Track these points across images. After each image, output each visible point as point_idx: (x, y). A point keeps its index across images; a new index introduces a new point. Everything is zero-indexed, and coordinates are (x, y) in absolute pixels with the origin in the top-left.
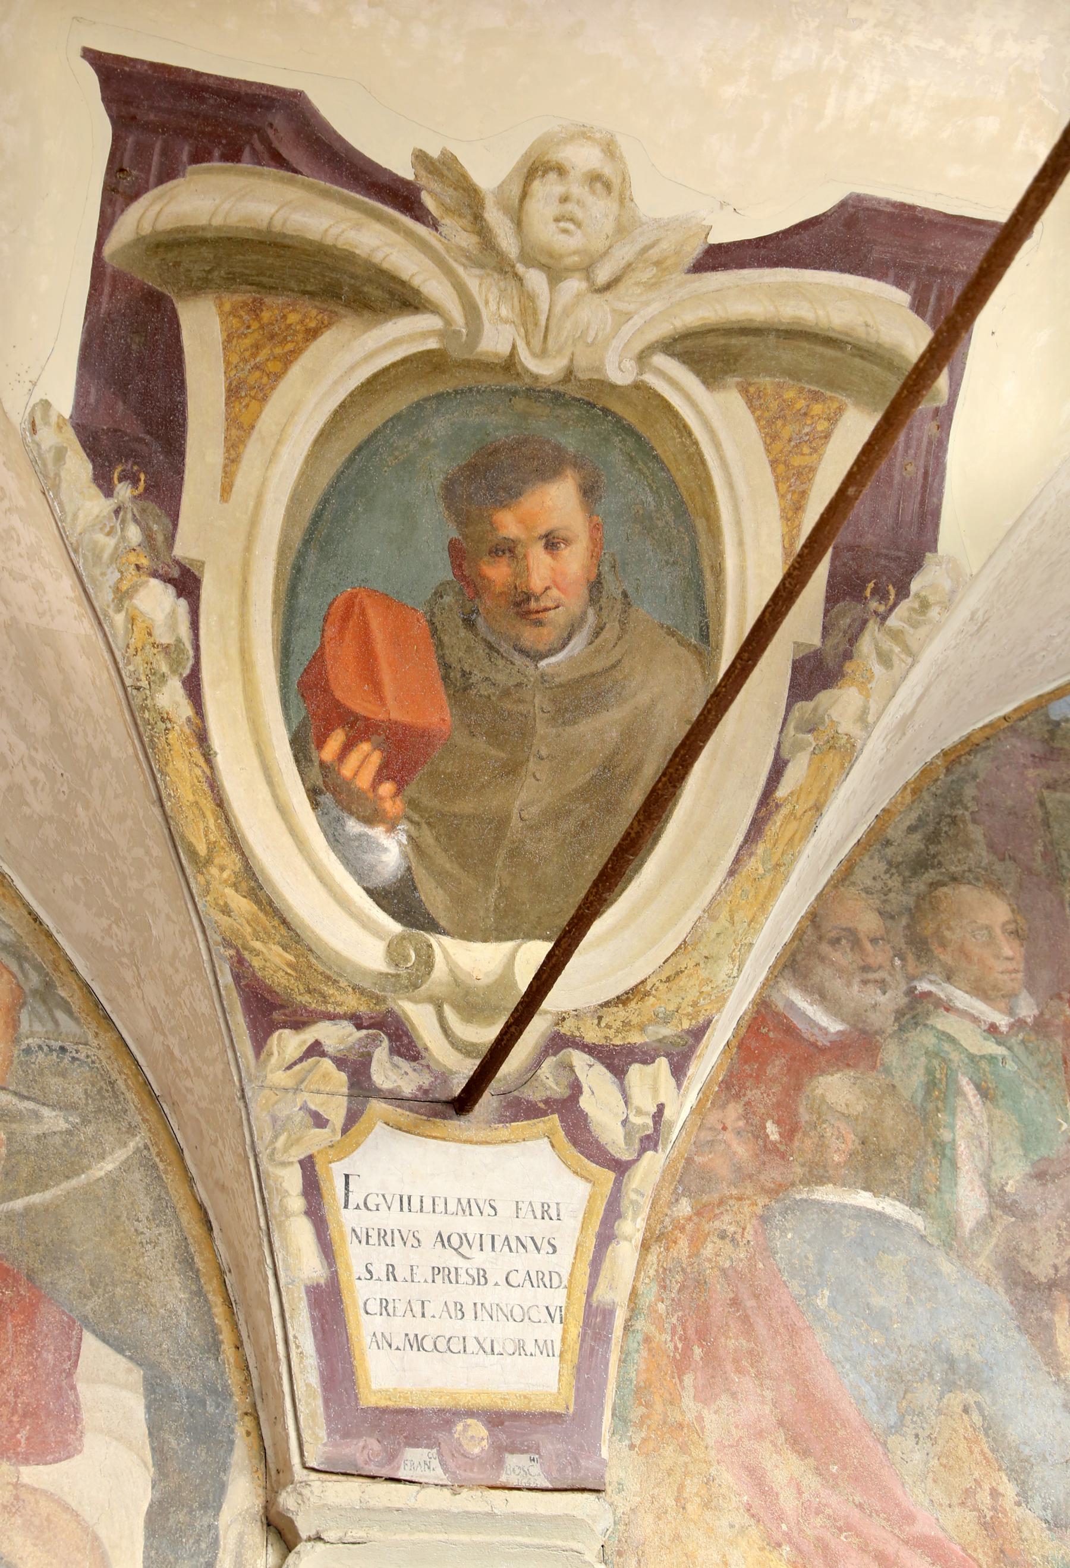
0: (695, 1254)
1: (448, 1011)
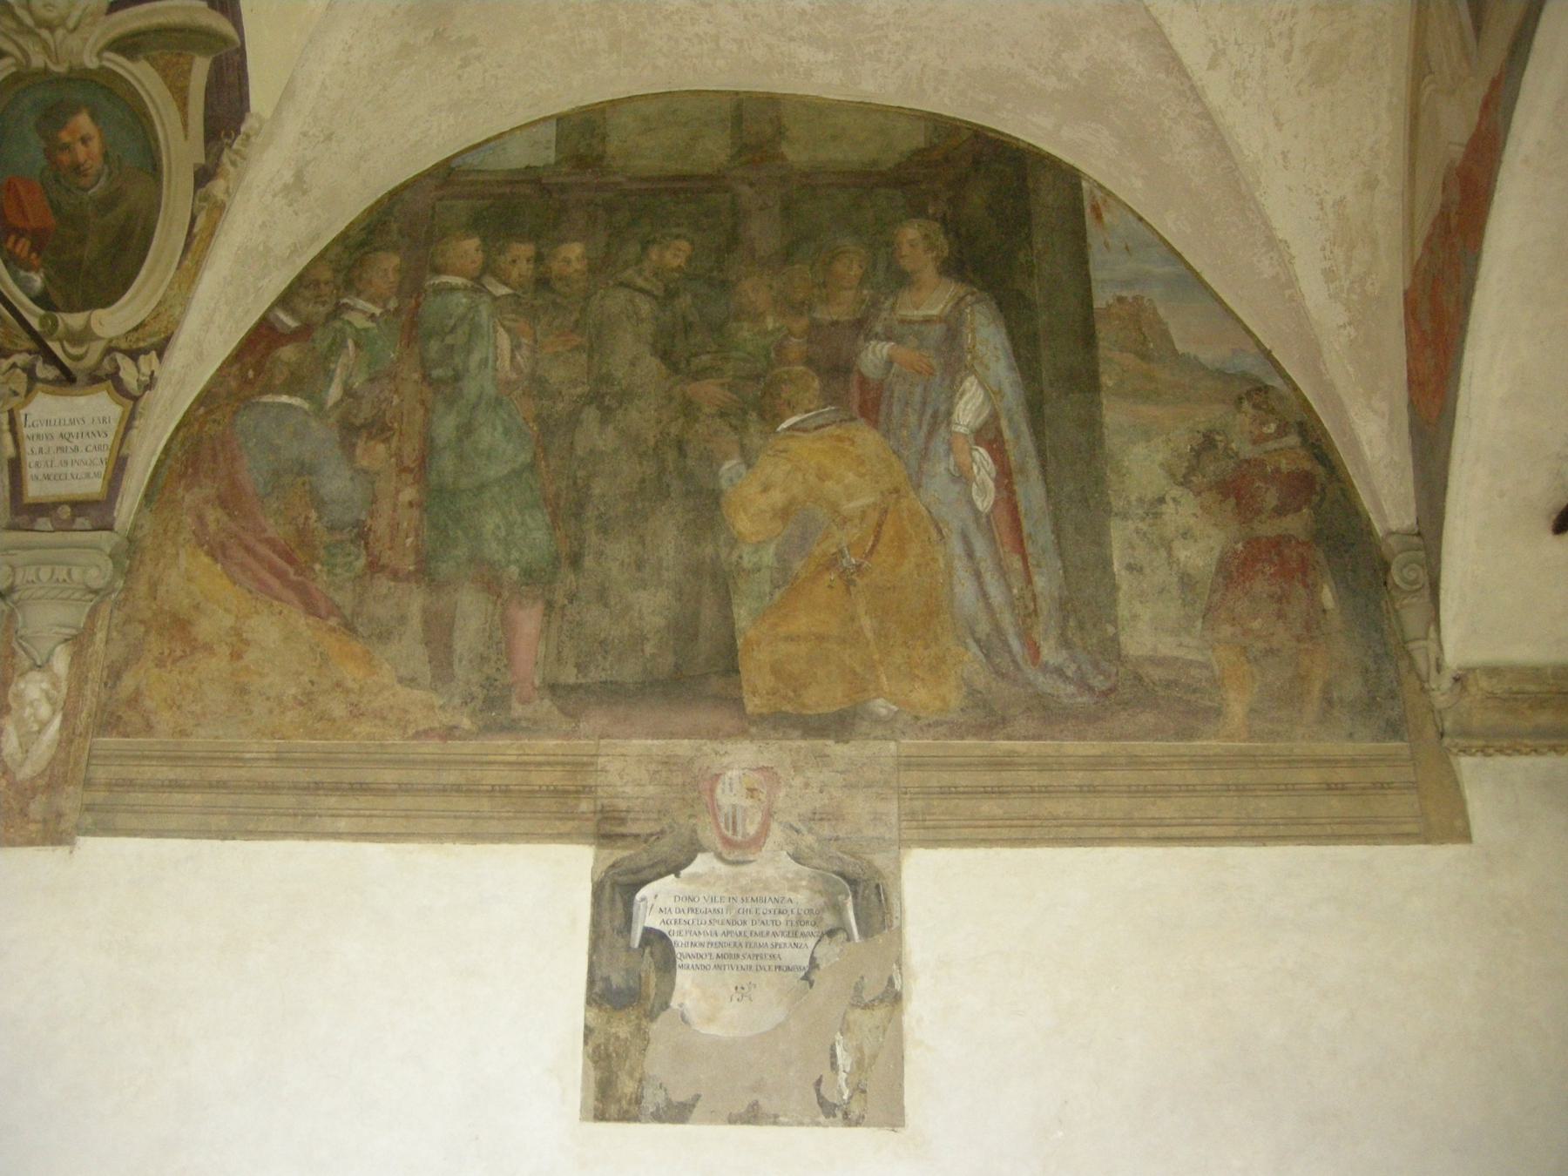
1: (66, 344)
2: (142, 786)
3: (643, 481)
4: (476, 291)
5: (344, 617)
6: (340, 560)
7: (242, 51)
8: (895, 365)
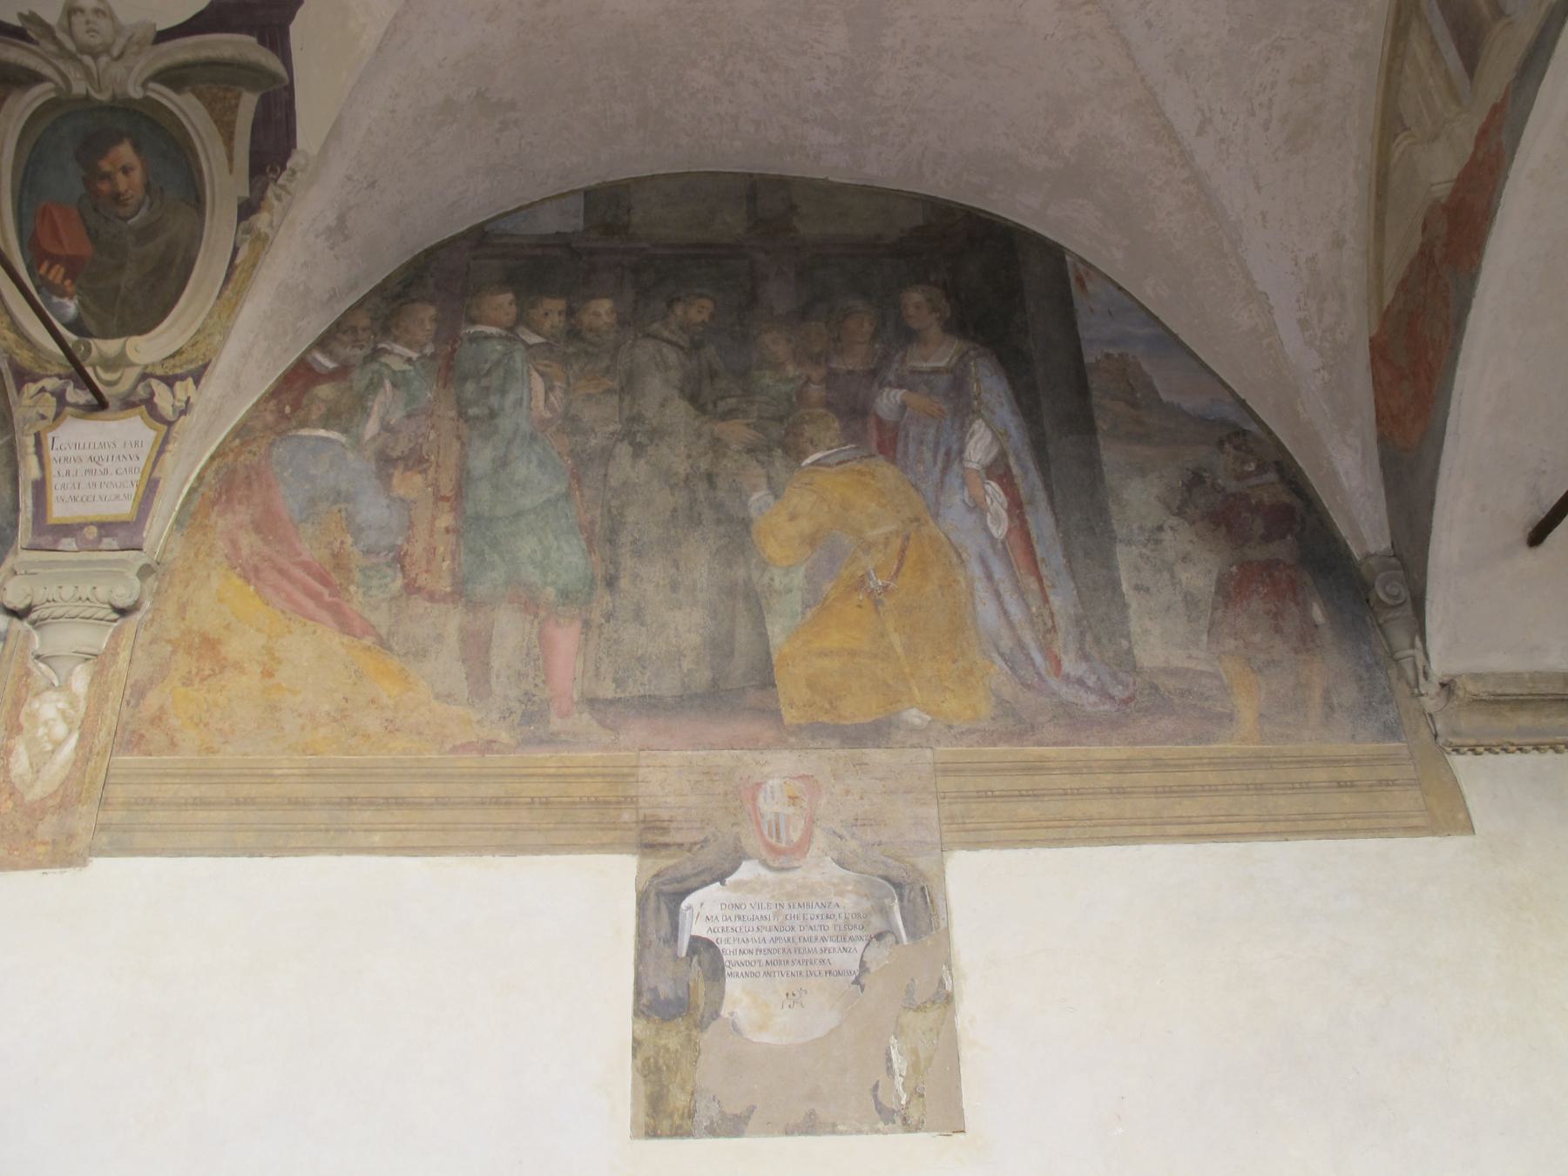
0: (235, 460)
1: (99, 370)
2: (163, 804)
3: (675, 510)
4: (508, 339)
5: (379, 636)
6: (375, 583)
7: (290, 89)
8: (909, 409)
